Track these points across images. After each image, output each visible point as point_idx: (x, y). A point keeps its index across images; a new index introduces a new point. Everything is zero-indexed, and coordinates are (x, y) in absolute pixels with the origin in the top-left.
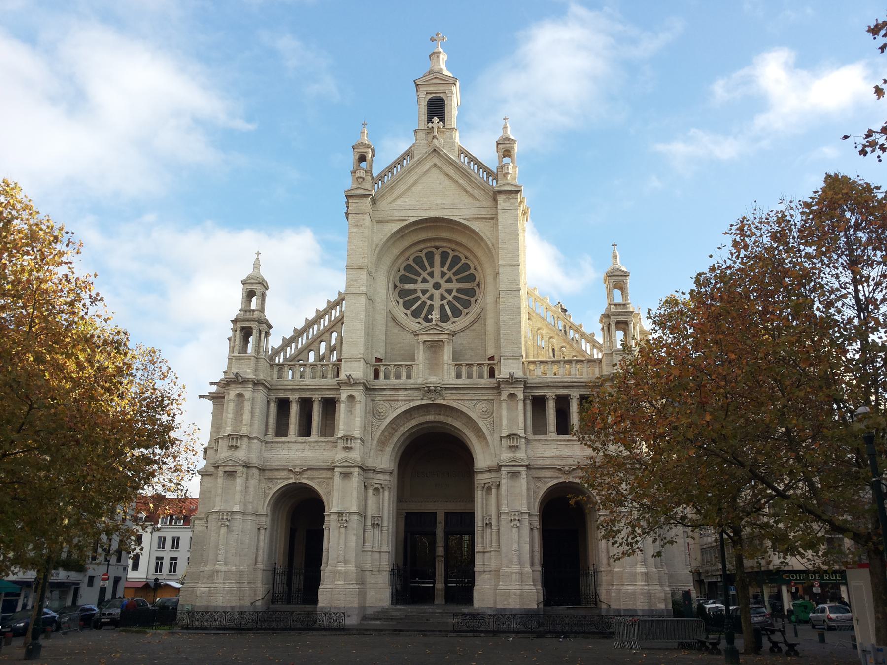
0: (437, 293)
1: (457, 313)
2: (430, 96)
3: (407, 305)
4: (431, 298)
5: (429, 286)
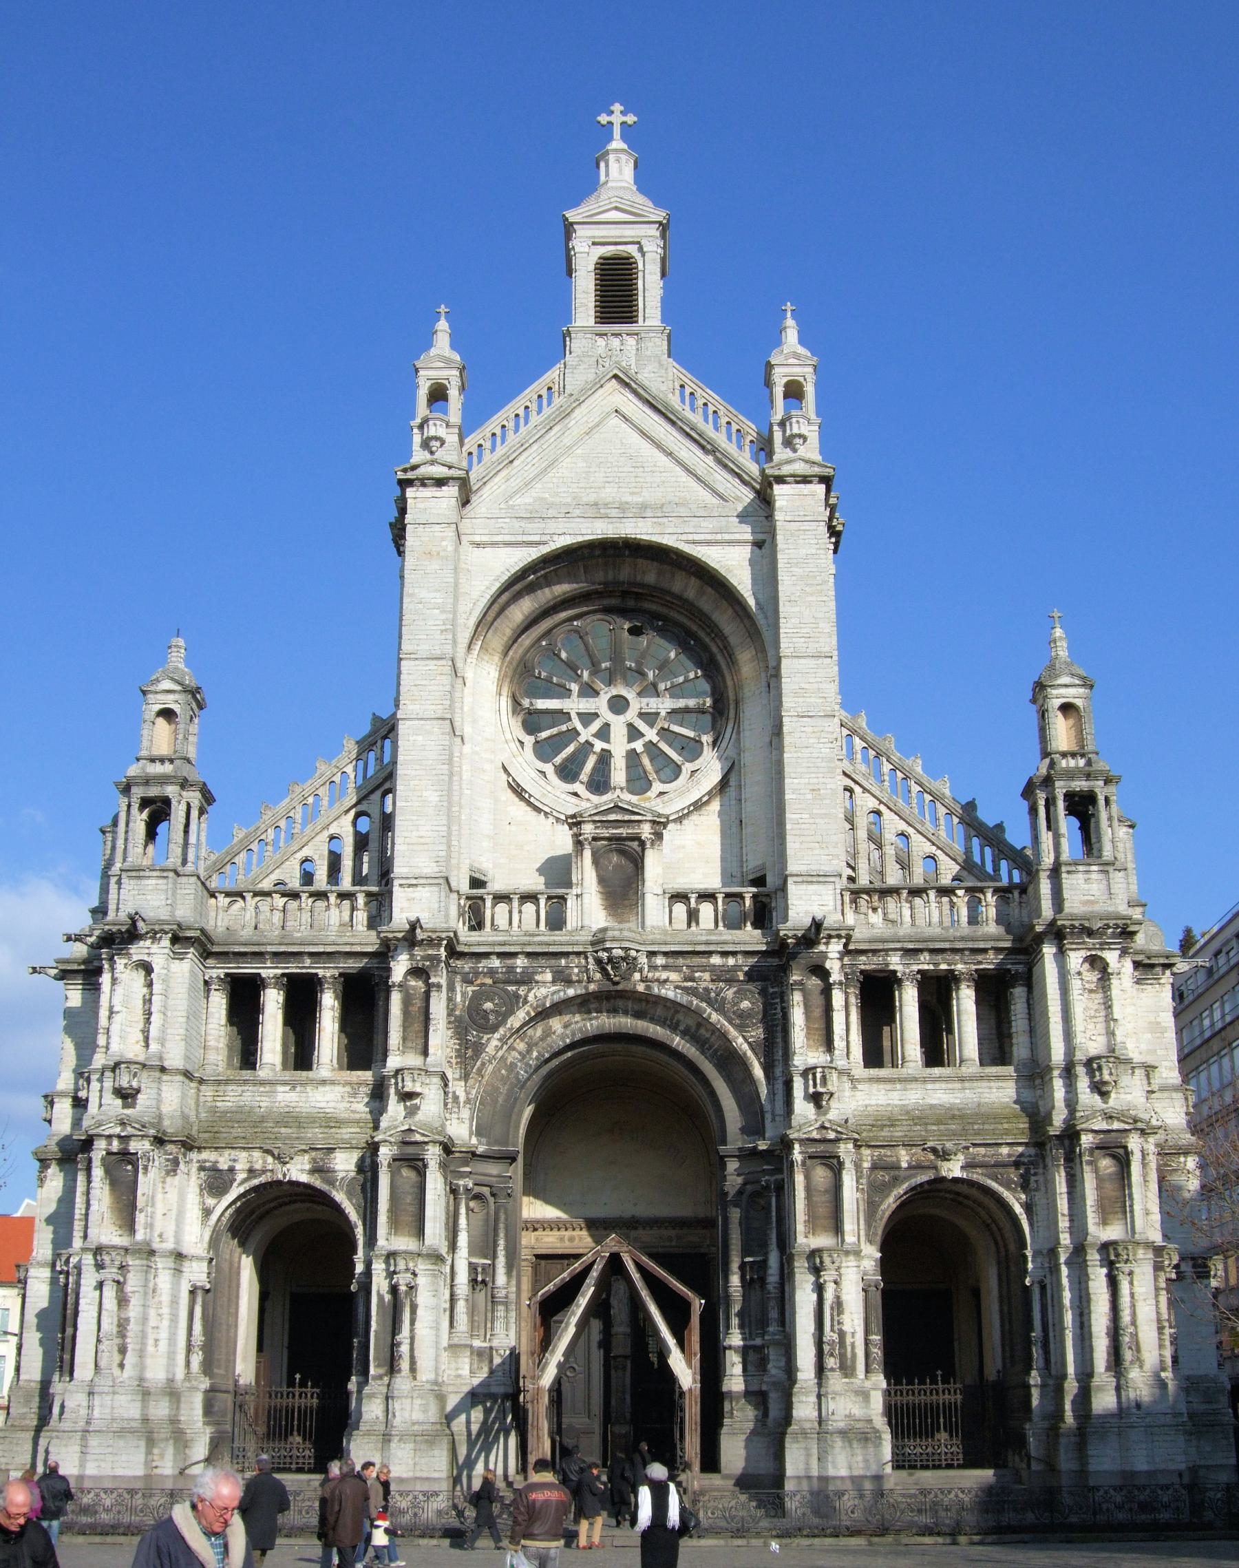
3: (544, 751)
4: (604, 733)
5: (600, 704)
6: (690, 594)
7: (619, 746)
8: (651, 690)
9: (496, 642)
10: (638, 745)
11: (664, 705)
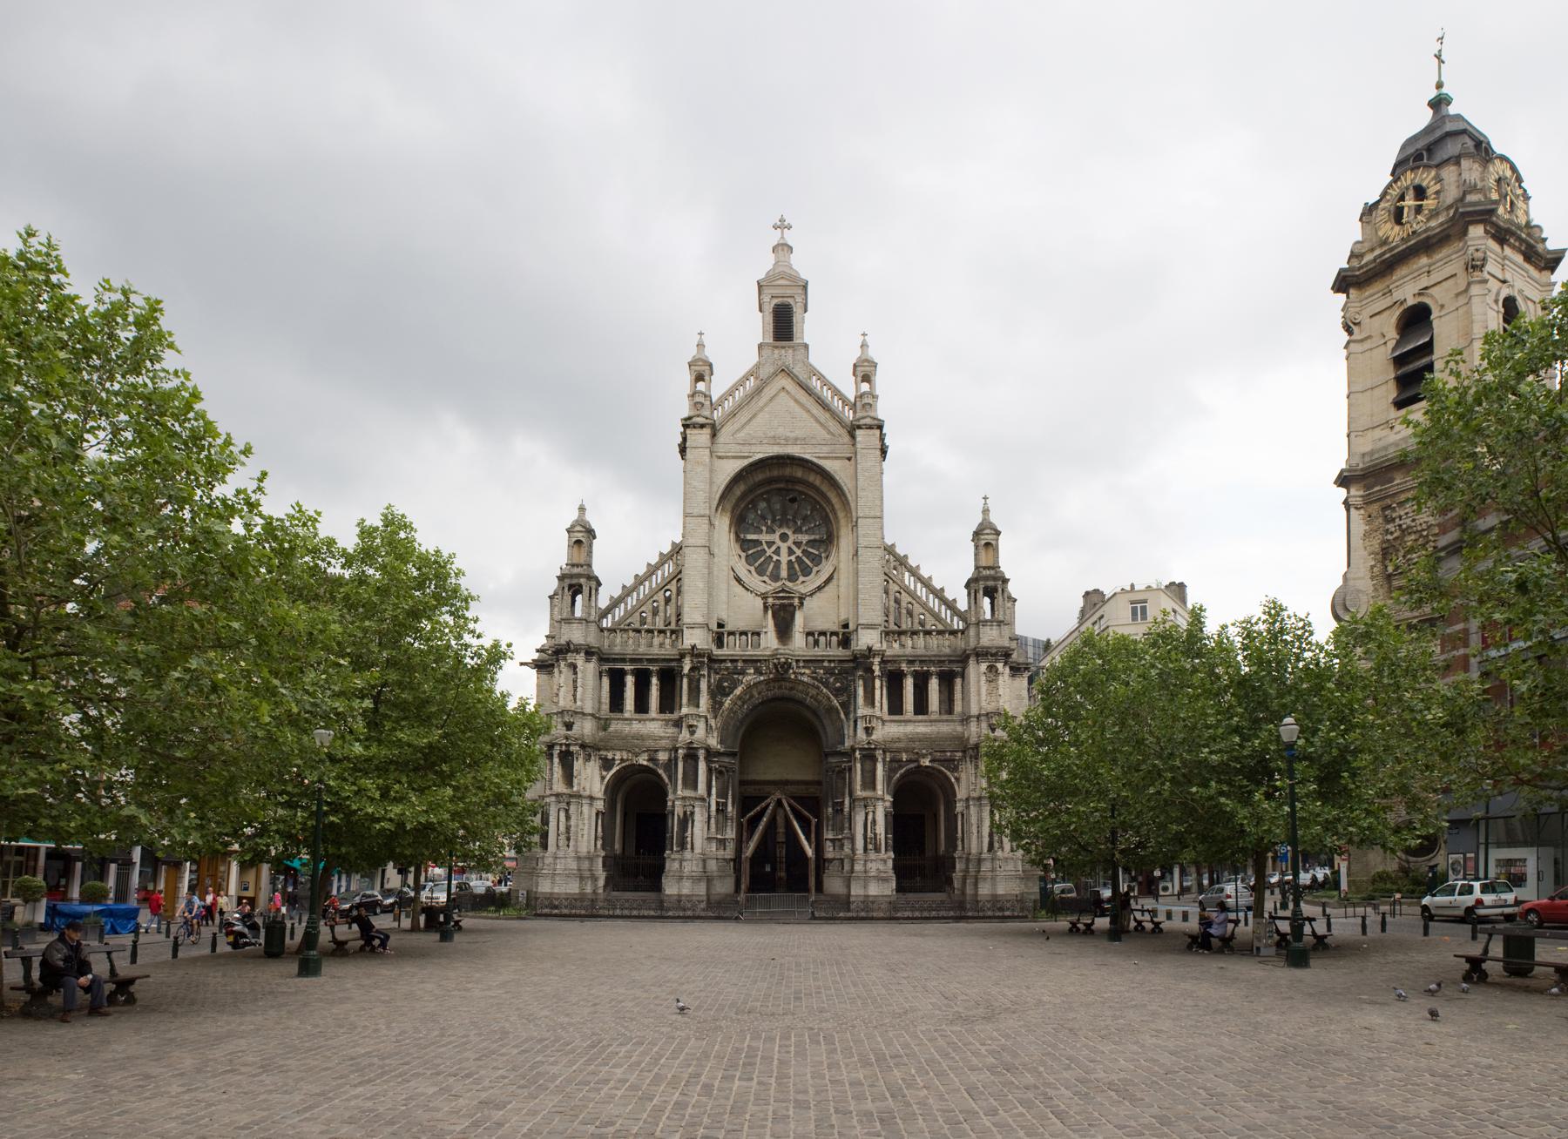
0: (784, 547)
1: (806, 572)
2: (776, 301)
3: (750, 560)
4: (777, 552)
5: (776, 537)
6: (818, 483)
7: (784, 558)
8: (798, 531)
9: (729, 507)
10: (793, 558)
11: (804, 538)
